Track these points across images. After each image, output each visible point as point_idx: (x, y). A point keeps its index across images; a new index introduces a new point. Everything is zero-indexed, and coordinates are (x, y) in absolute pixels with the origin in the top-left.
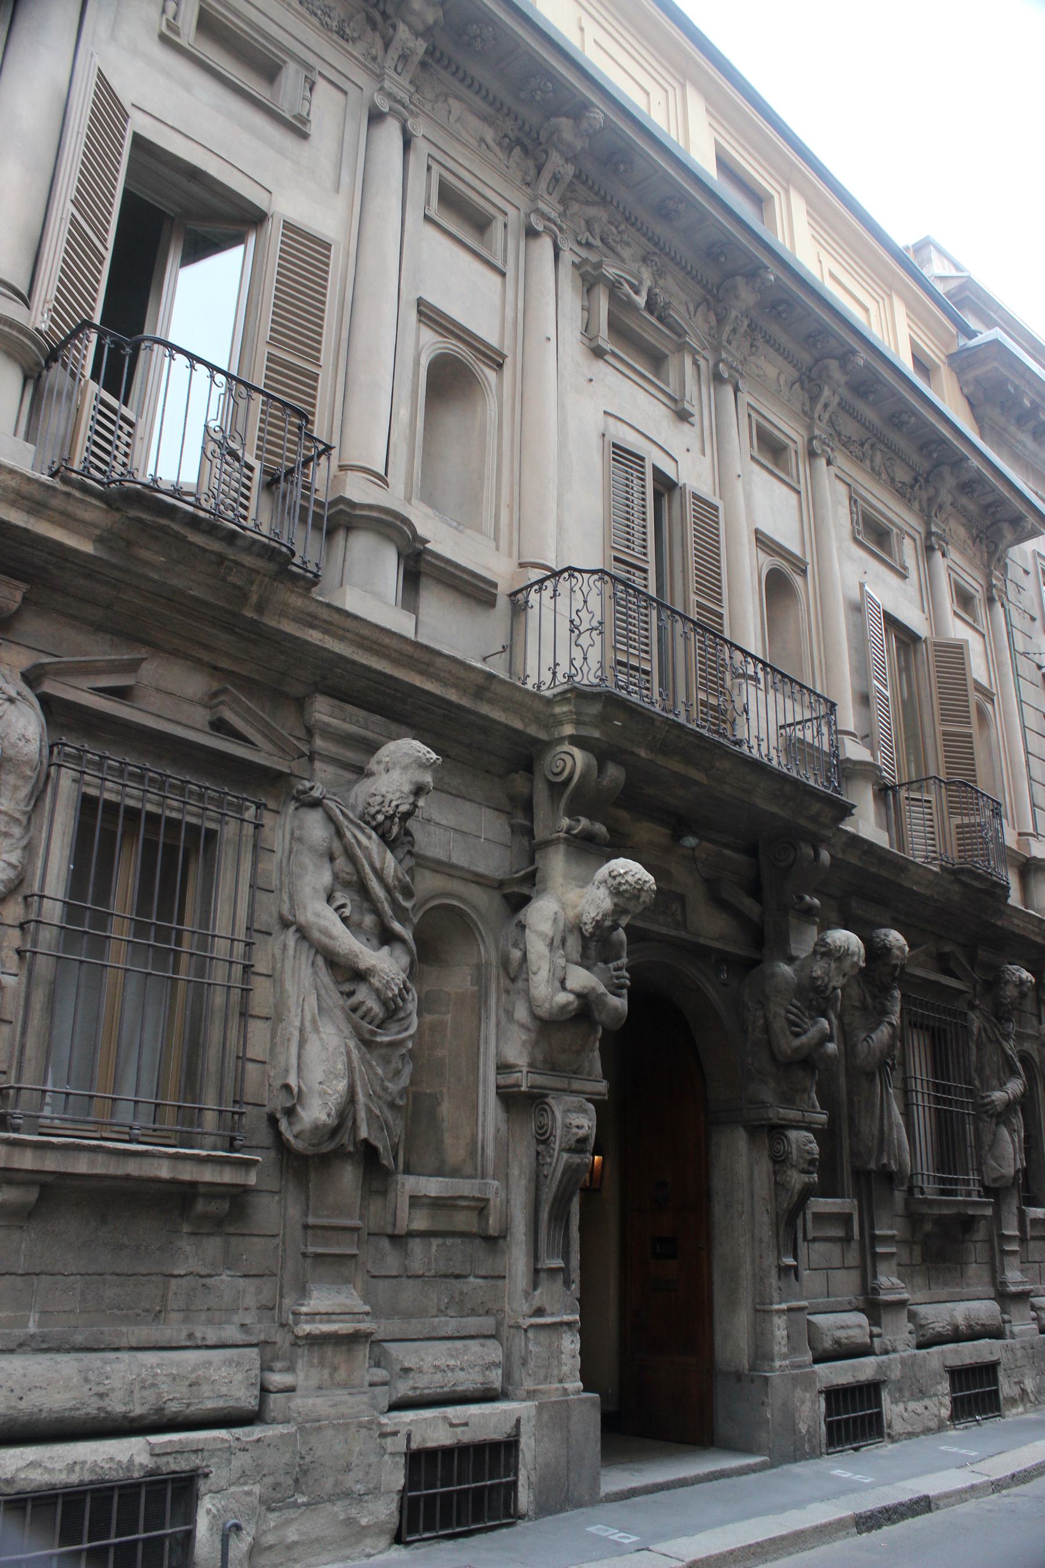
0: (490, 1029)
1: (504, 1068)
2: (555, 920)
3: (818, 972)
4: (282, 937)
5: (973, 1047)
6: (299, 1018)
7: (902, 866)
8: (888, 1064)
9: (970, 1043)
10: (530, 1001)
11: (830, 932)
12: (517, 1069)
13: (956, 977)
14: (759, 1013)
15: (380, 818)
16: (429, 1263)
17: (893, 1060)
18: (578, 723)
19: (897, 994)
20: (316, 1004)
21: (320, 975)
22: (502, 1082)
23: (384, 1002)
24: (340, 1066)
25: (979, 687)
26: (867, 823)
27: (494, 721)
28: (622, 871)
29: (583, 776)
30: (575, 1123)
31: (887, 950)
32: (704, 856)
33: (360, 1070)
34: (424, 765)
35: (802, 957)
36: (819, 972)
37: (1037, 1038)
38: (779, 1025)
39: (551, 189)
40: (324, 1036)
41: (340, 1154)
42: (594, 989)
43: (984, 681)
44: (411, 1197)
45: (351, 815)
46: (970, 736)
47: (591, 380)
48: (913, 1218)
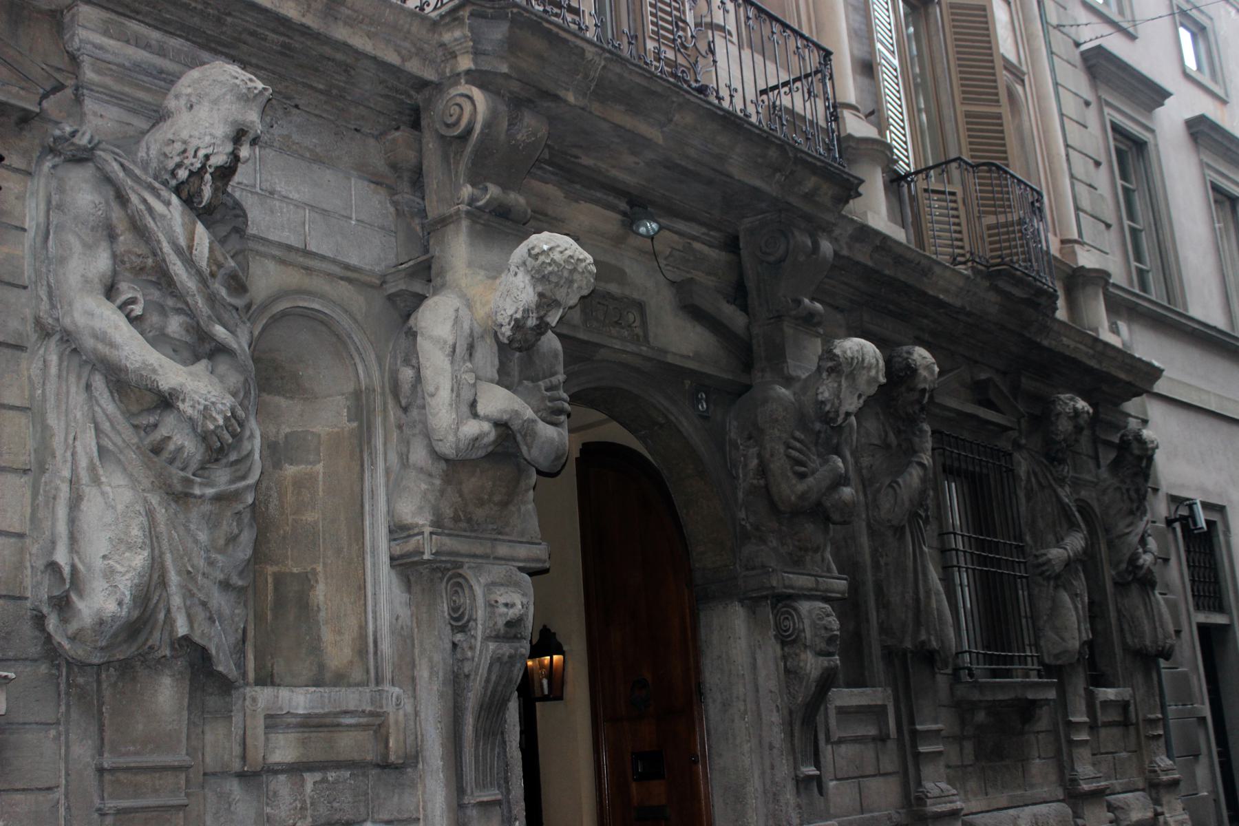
0: (377, 481)
1: (398, 530)
2: (457, 320)
3: (825, 393)
4: (41, 352)
5: (1022, 495)
6: (69, 465)
7: (926, 268)
8: (920, 516)
9: (1018, 491)
10: (427, 435)
11: (837, 342)
12: (416, 531)
13: (998, 410)
14: (753, 451)
15: (183, 174)
16: (303, 808)
17: (926, 510)
18: (477, 53)
19: (927, 427)
20: (94, 443)
21: (102, 402)
22: (398, 551)
23: (204, 437)
24: (135, 532)
25: (1008, 66)
26: (875, 209)
27: (359, 54)
28: (545, 247)
29: (488, 125)
30: (502, 600)
31: (911, 371)
32: (668, 251)
33: (171, 538)
34: (246, 98)
35: (803, 377)
36: (826, 394)
37: (1096, 484)
38: (778, 465)
40: (108, 489)
41: (149, 662)
42: (517, 413)
43: (1012, 57)
44: (268, 717)
45: (137, 172)
46: (999, 116)
48: (963, 709)
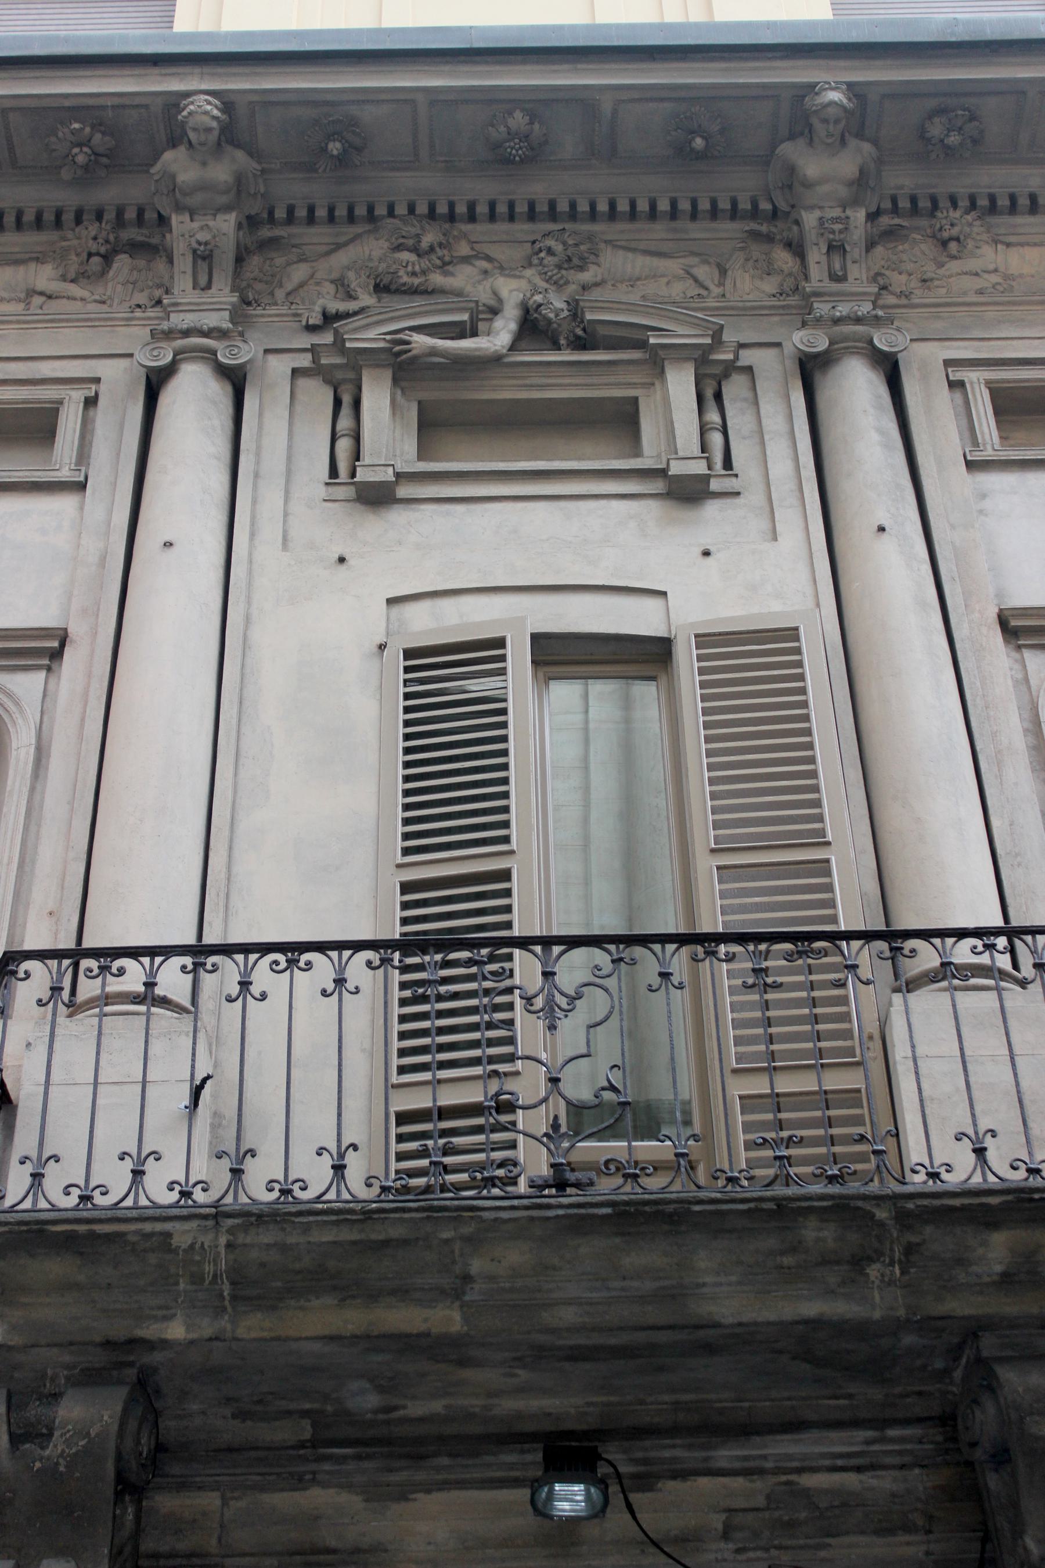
39: (203, 280)
47: (342, 560)
